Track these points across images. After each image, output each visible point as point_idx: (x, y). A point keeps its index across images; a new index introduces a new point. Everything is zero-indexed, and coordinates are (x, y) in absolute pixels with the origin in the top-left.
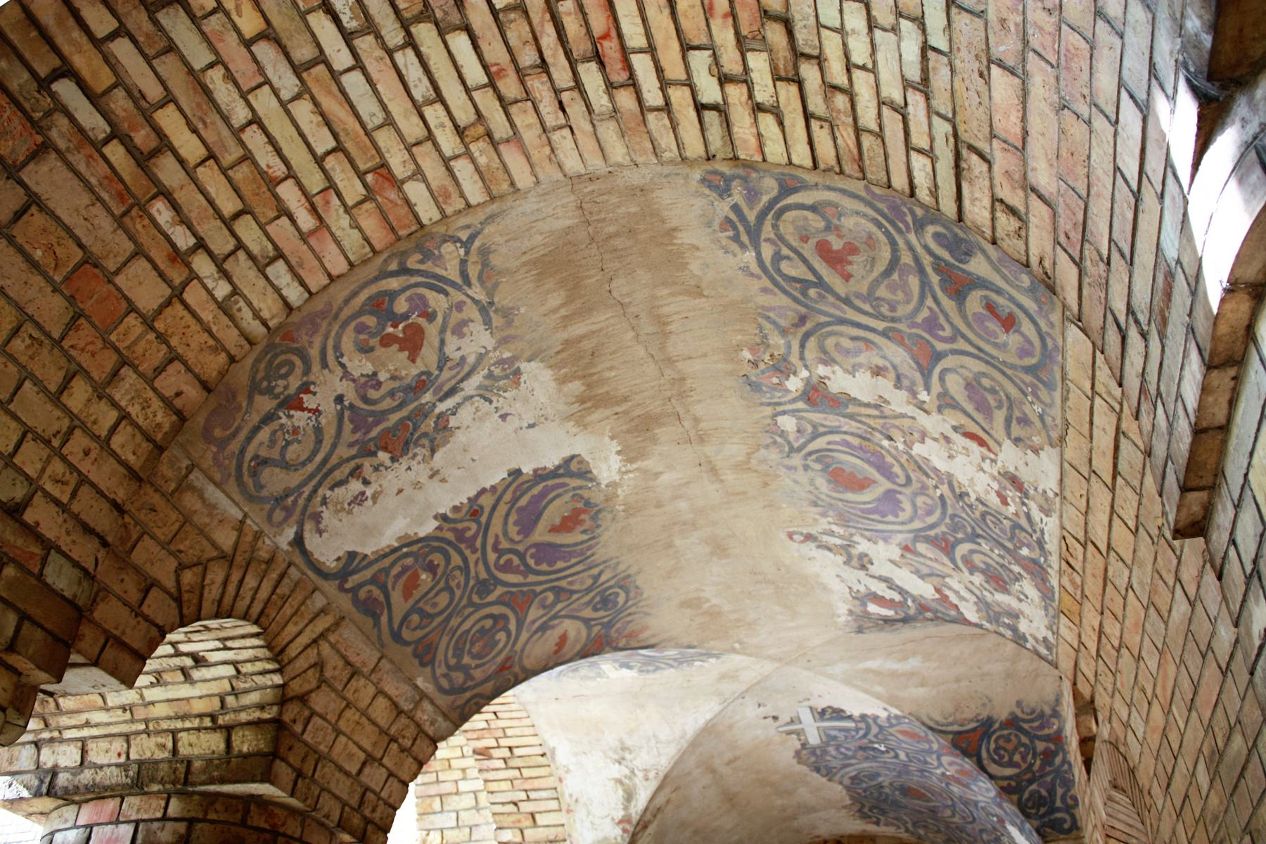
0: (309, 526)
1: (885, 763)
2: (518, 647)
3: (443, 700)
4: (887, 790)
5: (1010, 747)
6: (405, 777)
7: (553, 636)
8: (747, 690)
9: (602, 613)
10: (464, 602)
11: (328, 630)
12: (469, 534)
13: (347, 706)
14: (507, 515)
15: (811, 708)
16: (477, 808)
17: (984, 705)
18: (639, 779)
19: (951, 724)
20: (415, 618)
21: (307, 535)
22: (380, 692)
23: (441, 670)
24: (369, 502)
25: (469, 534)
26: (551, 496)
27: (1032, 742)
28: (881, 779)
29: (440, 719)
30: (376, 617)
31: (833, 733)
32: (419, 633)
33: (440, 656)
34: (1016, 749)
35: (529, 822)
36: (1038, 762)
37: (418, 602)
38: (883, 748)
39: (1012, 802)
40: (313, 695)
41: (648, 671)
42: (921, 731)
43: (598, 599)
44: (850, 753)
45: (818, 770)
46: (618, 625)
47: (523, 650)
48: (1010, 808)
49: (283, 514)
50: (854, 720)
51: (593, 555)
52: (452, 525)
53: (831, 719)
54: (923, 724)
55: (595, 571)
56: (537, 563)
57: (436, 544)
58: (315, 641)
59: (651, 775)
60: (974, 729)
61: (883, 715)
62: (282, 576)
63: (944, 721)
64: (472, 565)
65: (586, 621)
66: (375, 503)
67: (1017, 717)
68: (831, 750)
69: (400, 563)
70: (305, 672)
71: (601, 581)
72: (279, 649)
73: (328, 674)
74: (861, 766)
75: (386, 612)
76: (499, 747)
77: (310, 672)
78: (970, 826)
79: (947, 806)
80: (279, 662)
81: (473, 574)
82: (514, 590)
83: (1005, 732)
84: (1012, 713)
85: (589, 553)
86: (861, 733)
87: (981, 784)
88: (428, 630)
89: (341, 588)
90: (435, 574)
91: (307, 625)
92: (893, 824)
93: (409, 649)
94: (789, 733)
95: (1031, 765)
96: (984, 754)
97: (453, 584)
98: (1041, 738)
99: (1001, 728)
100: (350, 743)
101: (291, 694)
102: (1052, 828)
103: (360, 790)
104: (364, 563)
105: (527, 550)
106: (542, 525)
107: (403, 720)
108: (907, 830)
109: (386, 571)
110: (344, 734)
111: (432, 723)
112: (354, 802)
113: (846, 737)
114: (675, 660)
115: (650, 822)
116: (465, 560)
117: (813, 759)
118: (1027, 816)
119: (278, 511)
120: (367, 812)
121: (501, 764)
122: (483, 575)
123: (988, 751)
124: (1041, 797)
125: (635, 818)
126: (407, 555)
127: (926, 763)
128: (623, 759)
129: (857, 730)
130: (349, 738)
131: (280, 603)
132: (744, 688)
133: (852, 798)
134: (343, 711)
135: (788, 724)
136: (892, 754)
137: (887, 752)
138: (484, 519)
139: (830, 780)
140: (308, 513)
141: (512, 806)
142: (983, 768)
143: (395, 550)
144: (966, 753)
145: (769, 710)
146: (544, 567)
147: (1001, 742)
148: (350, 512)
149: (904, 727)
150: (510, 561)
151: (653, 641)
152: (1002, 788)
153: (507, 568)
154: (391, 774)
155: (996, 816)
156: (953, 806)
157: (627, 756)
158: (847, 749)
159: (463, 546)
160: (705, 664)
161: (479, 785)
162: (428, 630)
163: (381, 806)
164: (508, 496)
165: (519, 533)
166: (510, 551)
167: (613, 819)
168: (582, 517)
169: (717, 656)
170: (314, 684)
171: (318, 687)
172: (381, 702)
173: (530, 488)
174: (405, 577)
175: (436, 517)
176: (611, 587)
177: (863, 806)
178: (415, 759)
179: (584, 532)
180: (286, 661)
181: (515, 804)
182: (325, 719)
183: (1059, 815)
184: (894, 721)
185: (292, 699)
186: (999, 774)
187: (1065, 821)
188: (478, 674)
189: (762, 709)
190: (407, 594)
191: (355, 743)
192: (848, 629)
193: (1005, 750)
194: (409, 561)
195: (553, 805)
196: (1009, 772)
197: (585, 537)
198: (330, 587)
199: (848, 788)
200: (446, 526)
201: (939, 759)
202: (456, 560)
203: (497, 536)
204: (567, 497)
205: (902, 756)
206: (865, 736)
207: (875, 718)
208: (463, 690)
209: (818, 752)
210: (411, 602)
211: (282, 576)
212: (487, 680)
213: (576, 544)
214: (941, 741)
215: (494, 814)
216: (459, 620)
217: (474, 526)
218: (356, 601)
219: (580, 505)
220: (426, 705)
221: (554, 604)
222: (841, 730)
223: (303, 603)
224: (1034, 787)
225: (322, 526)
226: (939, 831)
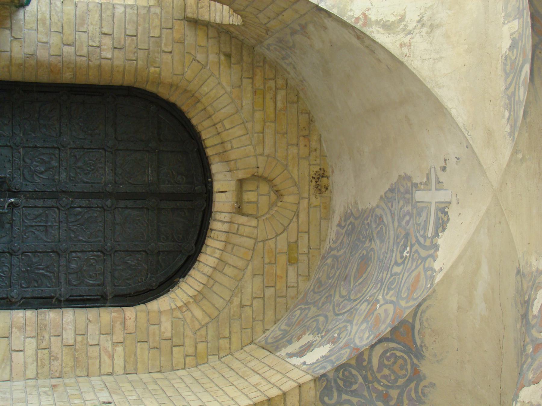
1: (392, 251)
4: (367, 244)
5: (396, 368)
8: (474, 152)
15: (450, 203)
17: (435, 355)
18: (402, 38)
19: (421, 323)
27: (398, 387)
28: (378, 242)
31: (424, 215)
34: (394, 372)
36: (381, 388)
38: (405, 254)
39: (350, 359)
41: (505, 64)
42: (419, 295)
44: (404, 223)
45: (391, 190)
48: (345, 356)
50: (433, 237)
53: (437, 218)
54: (424, 300)
59: (405, 50)
60: (415, 343)
61: (436, 266)
63: (424, 319)
67: (421, 380)
68: (408, 208)
74: (391, 229)
78: (331, 308)
79: (349, 293)
83: (409, 367)
84: (425, 377)
86: (422, 240)
87: (367, 335)
92: (337, 239)
94: (428, 176)
95: (379, 382)
96: (392, 345)
98: (400, 395)
99: (413, 364)
102: (326, 388)
108: (331, 249)
113: (419, 225)
114: (514, 94)
115: (363, 42)
117: (402, 190)
118: (337, 369)
123: (394, 349)
124: (351, 384)
125: (367, 31)
127: (389, 289)
128: (423, 26)
129: (425, 237)
132: (476, 150)
133: (364, 211)
135: (437, 178)
136: (400, 261)
137: (402, 257)
139: (381, 198)
142: (380, 341)
144: (394, 330)
145: (452, 165)
147: (400, 362)
149: (422, 281)
152: (362, 354)
155: (339, 338)
156: (349, 299)
157: (425, 30)
158: (408, 222)
160: (504, 121)
169: (512, 134)
177: (356, 219)
183: (335, 395)
184: (429, 273)
186: (374, 353)
187: (330, 399)
192: (522, 264)
193: (394, 363)
196: (375, 362)
199: (373, 210)
201: (392, 302)
205: (397, 269)
206: (418, 241)
207: (434, 258)
209: (408, 196)
214: (408, 312)
222: (426, 222)
224: (360, 380)
226: (329, 278)
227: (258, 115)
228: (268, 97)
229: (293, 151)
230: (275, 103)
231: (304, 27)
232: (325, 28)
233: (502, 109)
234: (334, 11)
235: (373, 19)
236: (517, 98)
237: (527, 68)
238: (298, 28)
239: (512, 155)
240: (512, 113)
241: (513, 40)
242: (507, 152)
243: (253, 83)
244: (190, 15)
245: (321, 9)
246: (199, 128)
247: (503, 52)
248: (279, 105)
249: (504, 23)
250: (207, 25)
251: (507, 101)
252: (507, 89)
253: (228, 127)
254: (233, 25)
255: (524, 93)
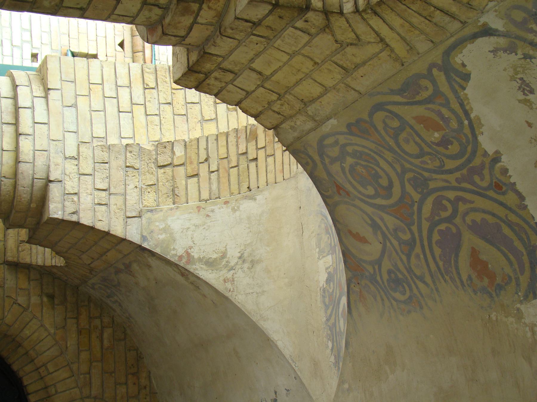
0: (502, 41)
2: (358, 203)
3: (313, 138)
6: (243, 105)
7: (367, 232)
8: (302, 383)
9: (385, 276)
10: (408, 166)
11: (392, 50)
12: (477, 179)
13: (316, 63)
14: (494, 215)
16: (204, 120)
20: (396, 124)
21: (493, 39)
22: (326, 90)
23: (342, 139)
24: (521, 97)
25: (477, 179)
26: (511, 257)
29: (296, 134)
30: (401, 92)
32: (380, 126)
33: (355, 140)
35: (190, 172)
37: (412, 128)
40: (330, 37)
41: (324, 297)
43: (400, 276)
46: (372, 288)
47: (355, 206)
49: (519, 19)
51: (445, 281)
52: (487, 166)
55: (428, 279)
56: (440, 232)
57: (469, 149)
58: (382, 40)
59: (229, 285)
62: (453, 16)
64: (444, 176)
65: (379, 262)
66: (520, 101)
69: (453, 117)
70: (353, 30)
71: (417, 281)
72: (378, 10)
73: (349, 50)
75: (404, 100)
76: (258, 149)
77: (352, 35)
80: (364, 11)
81: (435, 176)
82: (415, 208)
85: (447, 278)
88: (383, 132)
89: (433, 65)
90: (438, 144)
91: (399, 34)
93: (365, 117)
97: (426, 158)
100: (281, 64)
101: (333, 19)
103: (236, 69)
104: (457, 87)
105: (455, 225)
106: (480, 244)
107: (298, 105)
109: (447, 104)
110: (289, 60)
111: (292, 128)
112: (226, 65)
114: (334, 325)
115: (187, 279)
116: (450, 172)
119: (524, 15)
120: (216, 74)
121: (242, 149)
122: (432, 185)
125: (191, 268)
126: (461, 123)
128: (244, 261)
130: (285, 64)
131: (425, 13)
132: (304, 381)
134: (312, 60)
138: (491, 193)
140: (517, 41)
141: (205, 157)
143: (467, 114)
146: (436, 237)
148: (513, 79)
150: (445, 209)
151: (355, 313)
153: (438, 205)
154: (248, 94)
157: (246, 265)
159: (465, 171)
160: (328, 351)
161: (223, 128)
162: (383, 132)
163: (218, 84)
164: (513, 218)
165: (473, 221)
166: (455, 212)
167: (191, 248)
168: (486, 280)
169: (336, 363)
170: (339, 37)
171: (336, 41)
172: (317, 90)
173: (521, 239)
174: (437, 119)
175: (497, 152)
176: (411, 290)
178: (261, 113)
179: (470, 278)
180: (365, 16)
181: (206, 160)
182: (305, 45)
185: (328, 20)
188: (335, 168)
189: (285, 392)
190: (420, 120)
191: (280, 68)
194: (454, 124)
195: (205, 195)
197: (464, 278)
198: (436, 56)
200: (487, 161)
202: (450, 164)
203: (472, 202)
204: (508, 270)
208: (321, 154)
210: (412, 122)
211: (453, 16)
212: (329, 174)
213: (457, 268)
215: (198, 140)
216: (390, 160)
217: (484, 184)
218: (419, 76)
219: (499, 280)
220: (310, 125)
221: (398, 238)
223: (422, 32)
225: (501, 53)
227: (84, 356)
228: (94, 336)
229: (122, 390)
230: (102, 341)
231: (128, 267)
232: (149, 267)
233: (325, 339)
234: (158, 251)
235: (196, 256)
236: (338, 329)
237: (344, 300)
238: (122, 267)
239: (339, 385)
240: (335, 344)
241: (329, 273)
242: (334, 383)
243: (78, 323)
244: (10, 259)
245: (144, 249)
246: (21, 374)
247: (321, 285)
248: (106, 343)
249: (319, 258)
250: (28, 267)
251: (329, 332)
252: (328, 320)
253: (51, 370)
254: (56, 266)
255: (344, 325)
